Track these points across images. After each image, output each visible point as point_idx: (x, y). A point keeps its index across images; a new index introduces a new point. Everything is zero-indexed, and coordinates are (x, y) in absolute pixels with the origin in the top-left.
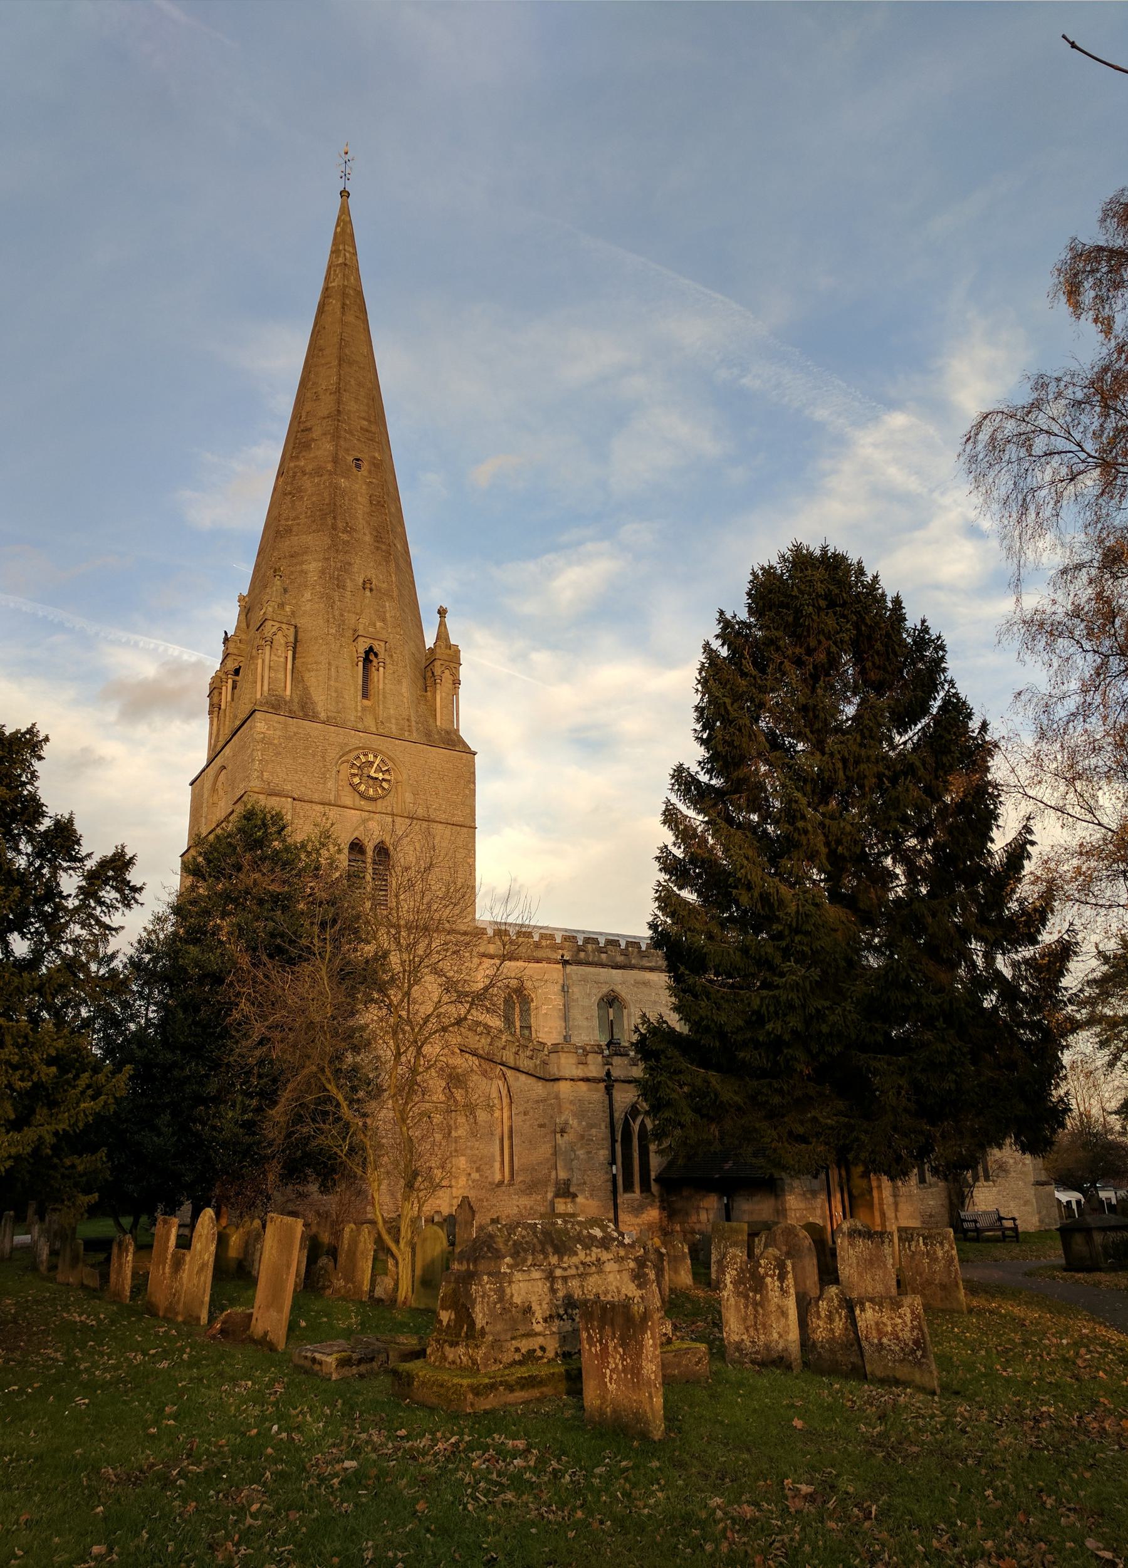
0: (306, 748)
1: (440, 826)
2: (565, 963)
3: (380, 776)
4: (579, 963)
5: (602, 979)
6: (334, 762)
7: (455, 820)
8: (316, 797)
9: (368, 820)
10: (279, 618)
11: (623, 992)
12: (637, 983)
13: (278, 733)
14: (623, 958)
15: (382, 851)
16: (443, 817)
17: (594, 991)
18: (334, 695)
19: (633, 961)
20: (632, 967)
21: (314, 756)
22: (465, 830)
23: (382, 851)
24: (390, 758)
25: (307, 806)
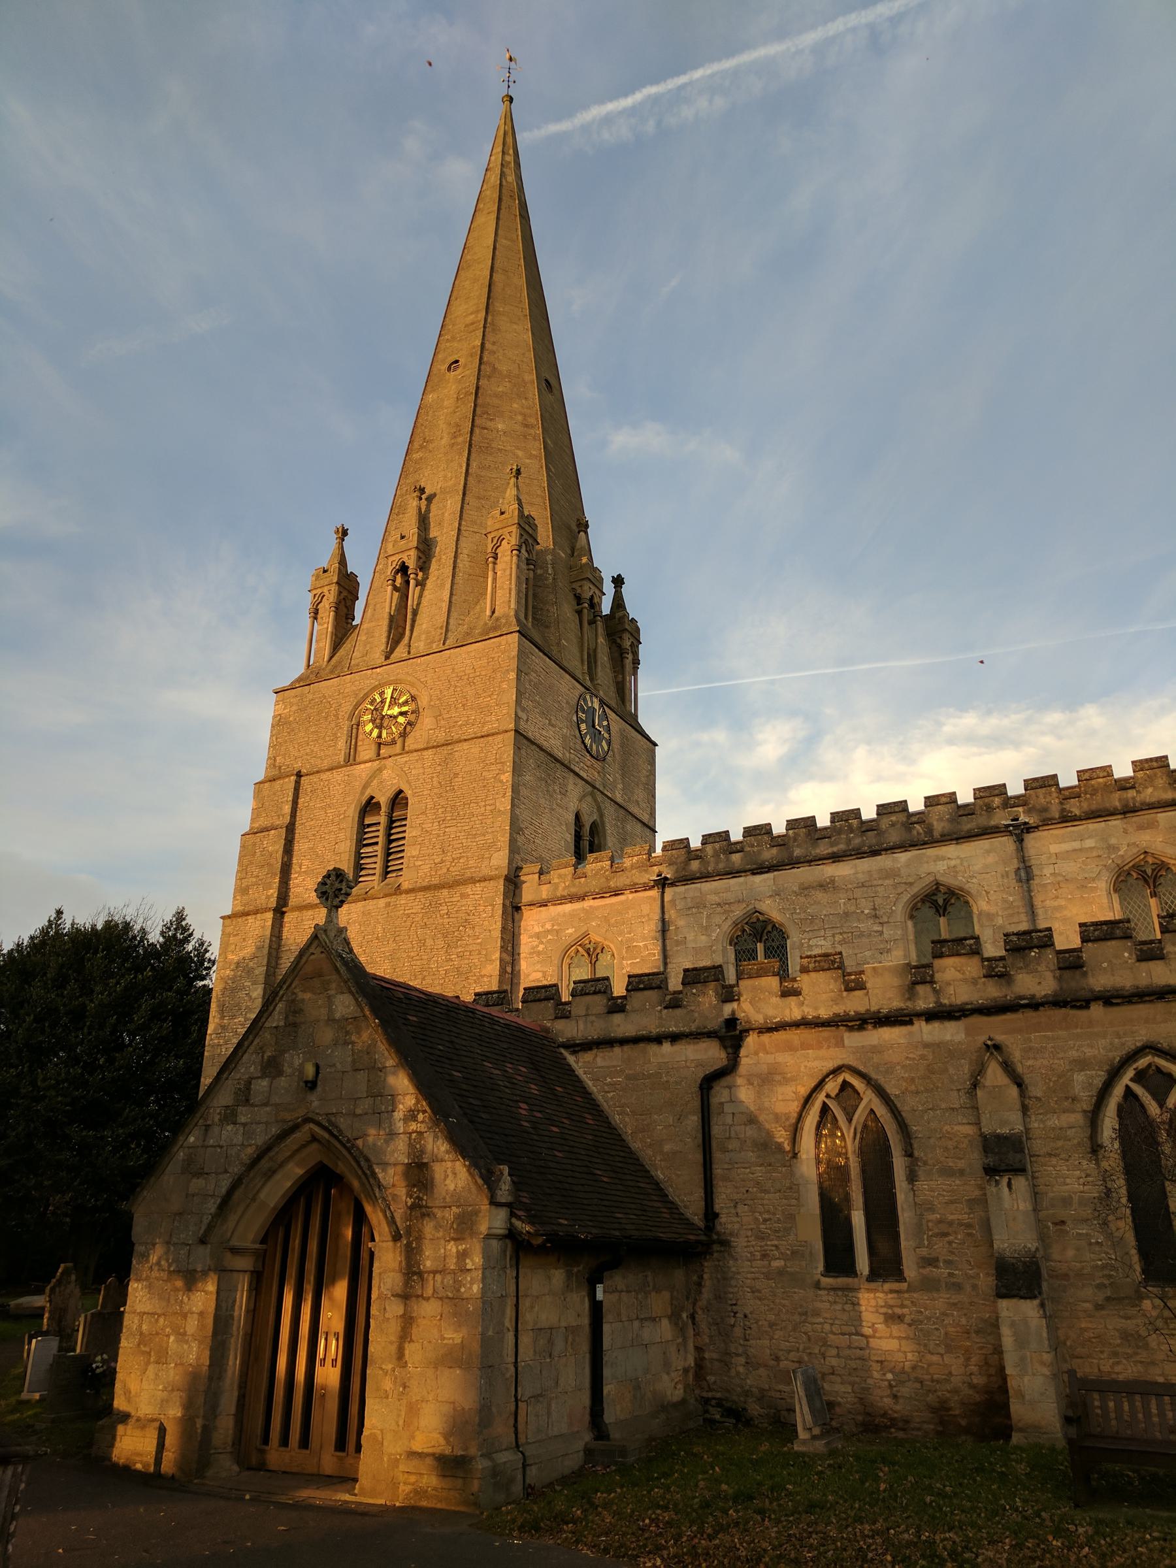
0: (319, 713)
1: (465, 745)
2: (662, 883)
3: (395, 711)
4: (687, 879)
5: (730, 897)
6: (347, 716)
7: (485, 730)
8: (326, 764)
9: (380, 770)
10: (322, 582)
11: (772, 910)
12: (805, 889)
13: (294, 708)
14: (774, 851)
15: (398, 800)
16: (471, 731)
17: (717, 919)
18: (364, 638)
19: (797, 852)
20: (794, 863)
21: (326, 718)
22: (500, 737)
23: (398, 800)
24: (412, 685)
25: (314, 778)
